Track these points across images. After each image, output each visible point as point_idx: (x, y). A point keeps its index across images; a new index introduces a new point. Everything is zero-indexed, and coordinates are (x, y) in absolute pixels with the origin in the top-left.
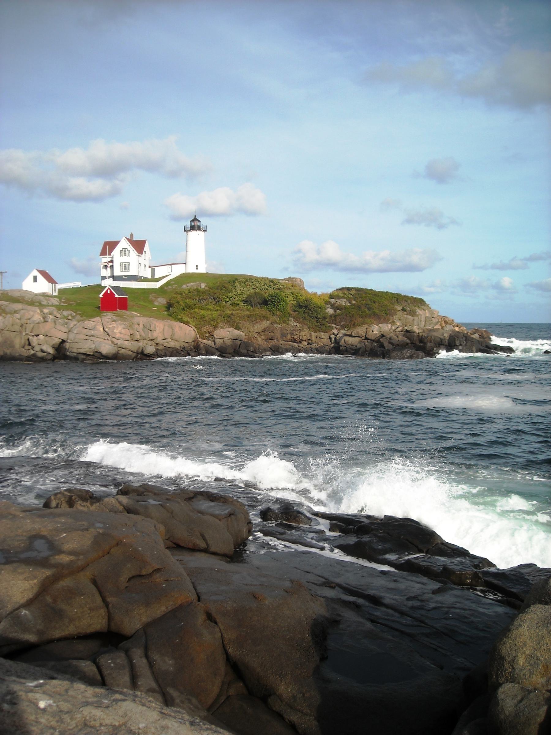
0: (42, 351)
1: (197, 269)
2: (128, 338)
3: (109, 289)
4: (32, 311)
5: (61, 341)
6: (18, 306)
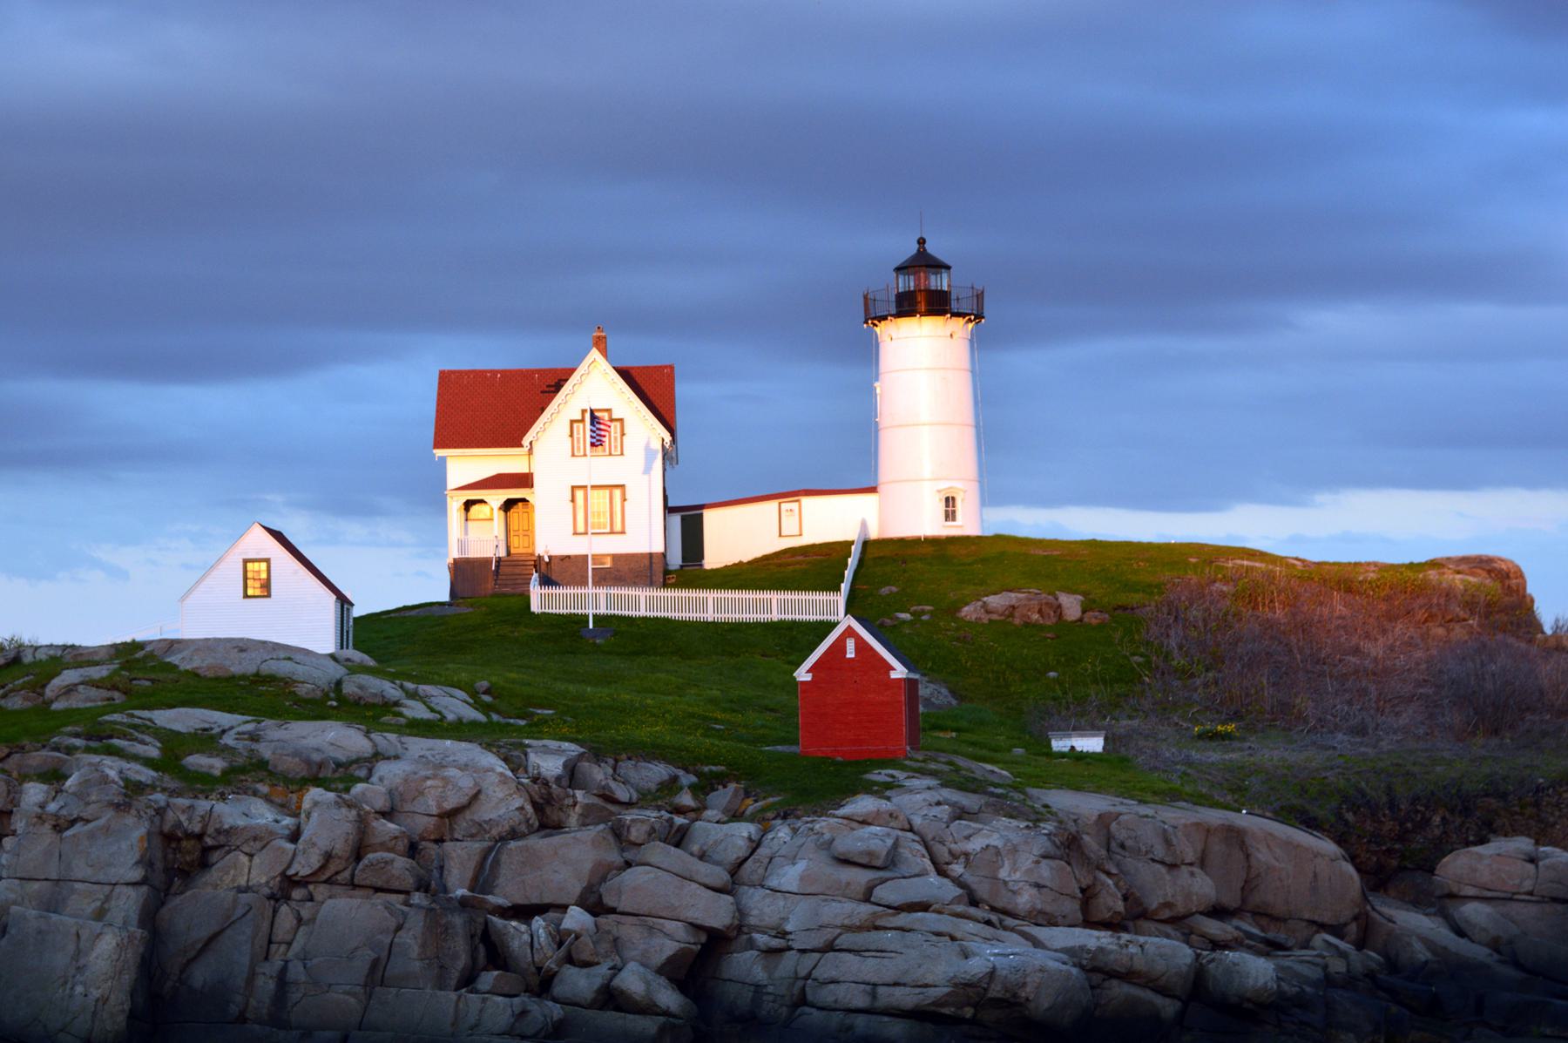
0: (610, 998)
1: (950, 515)
2: (1071, 907)
3: (849, 632)
4: (464, 767)
5: (703, 938)
6: (338, 738)
